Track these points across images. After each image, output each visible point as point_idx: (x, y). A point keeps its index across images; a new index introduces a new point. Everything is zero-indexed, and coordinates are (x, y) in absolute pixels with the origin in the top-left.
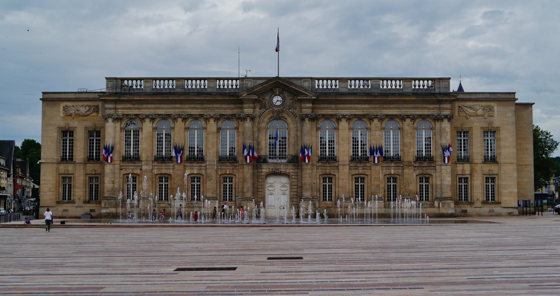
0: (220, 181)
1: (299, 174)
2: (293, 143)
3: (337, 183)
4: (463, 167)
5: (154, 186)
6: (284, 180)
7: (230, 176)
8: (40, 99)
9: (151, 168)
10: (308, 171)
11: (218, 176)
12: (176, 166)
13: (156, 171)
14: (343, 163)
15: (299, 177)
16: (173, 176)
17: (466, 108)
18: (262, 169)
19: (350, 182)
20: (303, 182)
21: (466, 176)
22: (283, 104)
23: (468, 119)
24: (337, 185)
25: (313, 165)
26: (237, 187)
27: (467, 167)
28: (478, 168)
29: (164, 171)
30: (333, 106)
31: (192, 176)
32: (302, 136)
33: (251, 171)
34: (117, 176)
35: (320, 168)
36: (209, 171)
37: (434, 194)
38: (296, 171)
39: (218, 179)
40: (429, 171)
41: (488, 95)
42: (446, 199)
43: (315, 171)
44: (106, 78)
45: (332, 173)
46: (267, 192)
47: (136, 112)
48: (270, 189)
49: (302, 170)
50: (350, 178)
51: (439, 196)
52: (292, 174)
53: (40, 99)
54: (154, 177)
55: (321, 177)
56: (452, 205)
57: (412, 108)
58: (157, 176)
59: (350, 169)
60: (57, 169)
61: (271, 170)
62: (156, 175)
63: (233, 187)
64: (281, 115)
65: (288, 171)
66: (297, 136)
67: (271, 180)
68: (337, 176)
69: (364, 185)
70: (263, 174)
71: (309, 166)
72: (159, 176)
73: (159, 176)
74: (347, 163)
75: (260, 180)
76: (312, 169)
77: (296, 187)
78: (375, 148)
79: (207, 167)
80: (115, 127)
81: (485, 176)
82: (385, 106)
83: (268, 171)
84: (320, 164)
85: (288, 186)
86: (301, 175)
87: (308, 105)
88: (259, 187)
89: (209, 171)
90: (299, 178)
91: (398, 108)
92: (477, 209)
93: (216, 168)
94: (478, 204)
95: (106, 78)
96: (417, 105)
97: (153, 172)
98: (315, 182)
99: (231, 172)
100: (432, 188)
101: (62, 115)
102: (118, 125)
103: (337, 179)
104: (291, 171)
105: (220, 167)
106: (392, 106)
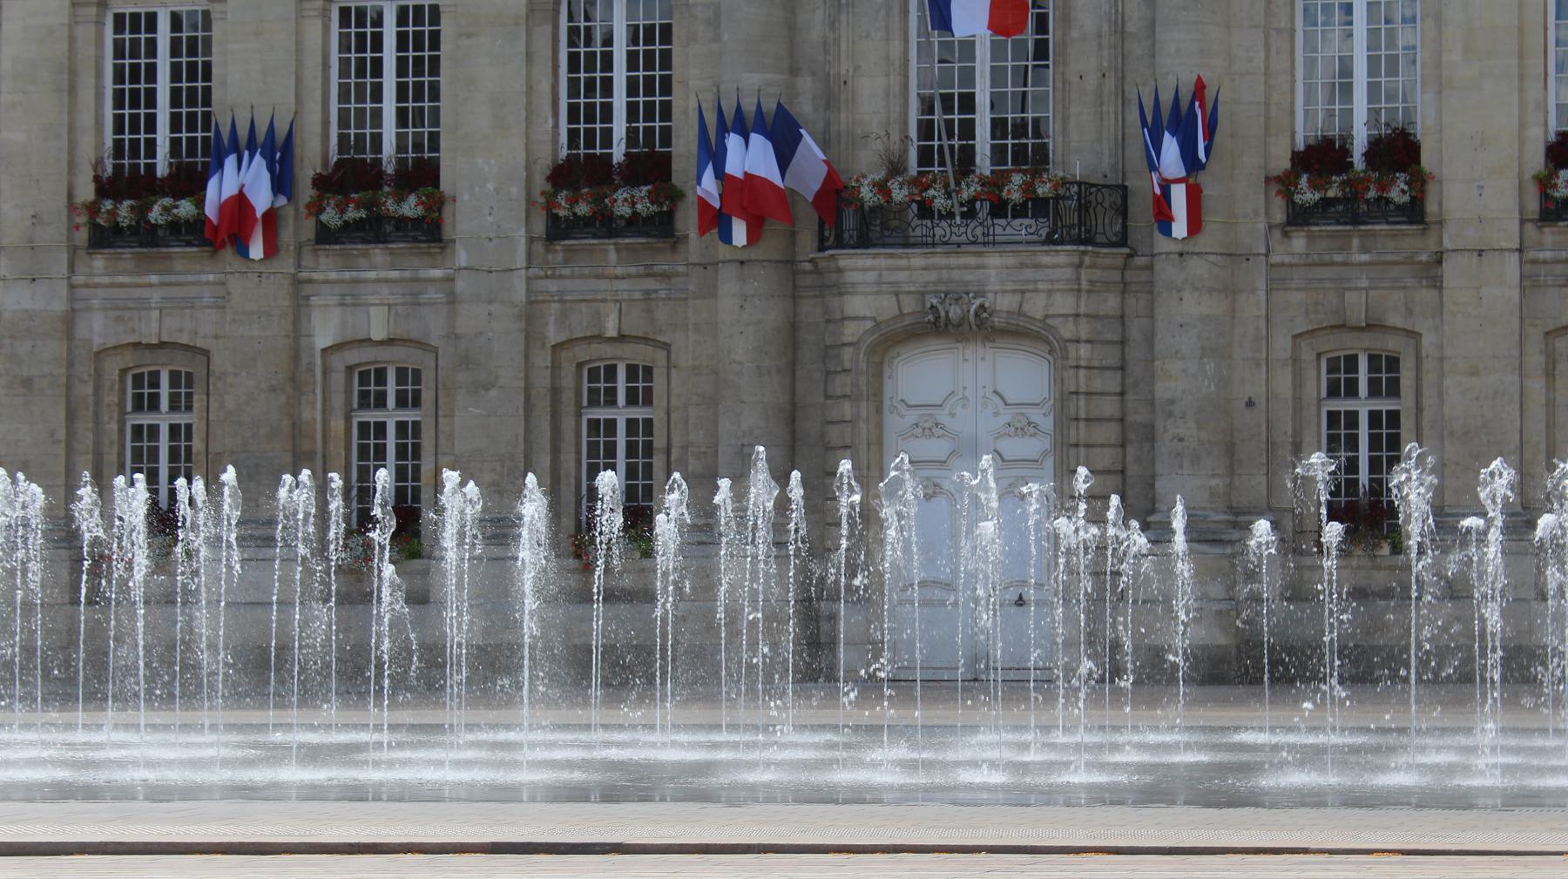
0: (555, 391)
1: (1135, 330)
2: (1092, 80)
3: (1429, 399)
5: (86, 438)
6: (1023, 376)
9: (59, 306)
10: (1192, 306)
11: (543, 359)
12: (235, 284)
13: (97, 329)
15: (1135, 353)
16: (220, 362)
18: (841, 290)
19: (1536, 386)
20: (1162, 390)
24: (1427, 415)
25: (1234, 256)
26: (676, 439)
29: (150, 330)
31: (353, 356)
32: (1152, 26)
33: (772, 314)
36: (471, 318)
38: (1111, 303)
39: (543, 381)
43: (1252, 306)
45: (1395, 320)
49: (1150, 288)
50: (1536, 359)
52: (1067, 330)
54: (84, 369)
55: (1308, 355)
58: (112, 367)
59: (1529, 283)
61: (909, 305)
62: (100, 354)
63: (659, 441)
65: (1036, 307)
66: (1120, 29)
67: (924, 375)
68: (1428, 341)
70: (851, 331)
71: (1198, 268)
72: (128, 359)
73: (128, 359)
74: (1508, 233)
75: (840, 384)
76: (1230, 291)
77: (1109, 432)
78: (243, 133)
79: (461, 285)
83: (885, 306)
84: (1299, 243)
85: (1047, 423)
86: (1150, 339)
88: (834, 434)
89: (471, 318)
90: (1127, 355)
93: (520, 294)
97: (81, 331)
98: (1256, 389)
99: (636, 323)
103: (1427, 365)
104: (1064, 304)
105: (553, 286)
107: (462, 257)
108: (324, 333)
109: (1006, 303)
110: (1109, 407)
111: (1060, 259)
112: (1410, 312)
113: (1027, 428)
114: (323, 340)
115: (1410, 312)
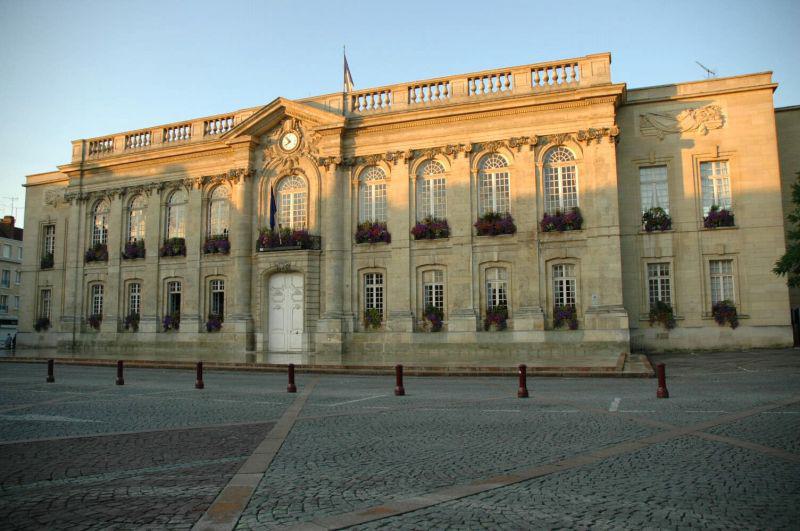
4: (657, 242)
6: (298, 281)
7: (219, 278)
8: (24, 186)
13: (125, 276)
14: (398, 245)
17: (658, 119)
19: (414, 280)
21: (662, 260)
22: (299, 148)
23: (662, 139)
27: (665, 240)
28: (691, 241)
30: (381, 138)
34: (80, 284)
35: (358, 256)
37: (587, 298)
39: (203, 284)
40: (572, 252)
41: (706, 85)
42: (608, 310)
44: (73, 142)
45: (381, 265)
46: (273, 305)
47: (104, 187)
48: (277, 298)
50: (414, 275)
51: (595, 304)
53: (24, 186)
54: (122, 284)
56: (625, 323)
57: (532, 124)
60: (37, 280)
64: (296, 166)
65: (299, 264)
67: (279, 281)
69: (441, 287)
73: (131, 282)
80: (80, 212)
81: (707, 259)
82: (476, 126)
83: (267, 266)
87: (333, 142)
91: (505, 128)
92: (693, 331)
94: (696, 319)
95: (73, 142)
96: (541, 117)
100: (581, 287)
101: (44, 204)
102: (84, 207)
106: (490, 125)
107: (188, 257)
108: (163, 276)
109: (293, 263)
110: (316, 287)
111: (305, 253)
112: (384, 263)
113: (297, 293)
114: (163, 276)
115: (384, 263)
